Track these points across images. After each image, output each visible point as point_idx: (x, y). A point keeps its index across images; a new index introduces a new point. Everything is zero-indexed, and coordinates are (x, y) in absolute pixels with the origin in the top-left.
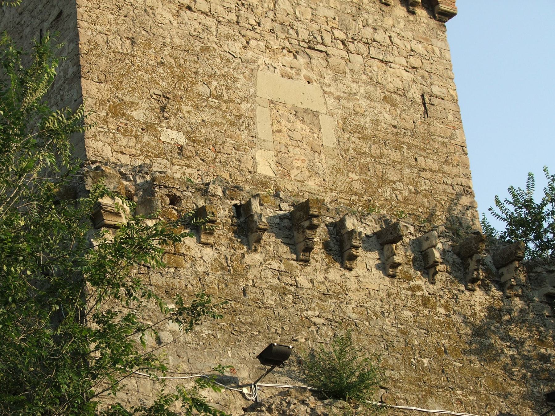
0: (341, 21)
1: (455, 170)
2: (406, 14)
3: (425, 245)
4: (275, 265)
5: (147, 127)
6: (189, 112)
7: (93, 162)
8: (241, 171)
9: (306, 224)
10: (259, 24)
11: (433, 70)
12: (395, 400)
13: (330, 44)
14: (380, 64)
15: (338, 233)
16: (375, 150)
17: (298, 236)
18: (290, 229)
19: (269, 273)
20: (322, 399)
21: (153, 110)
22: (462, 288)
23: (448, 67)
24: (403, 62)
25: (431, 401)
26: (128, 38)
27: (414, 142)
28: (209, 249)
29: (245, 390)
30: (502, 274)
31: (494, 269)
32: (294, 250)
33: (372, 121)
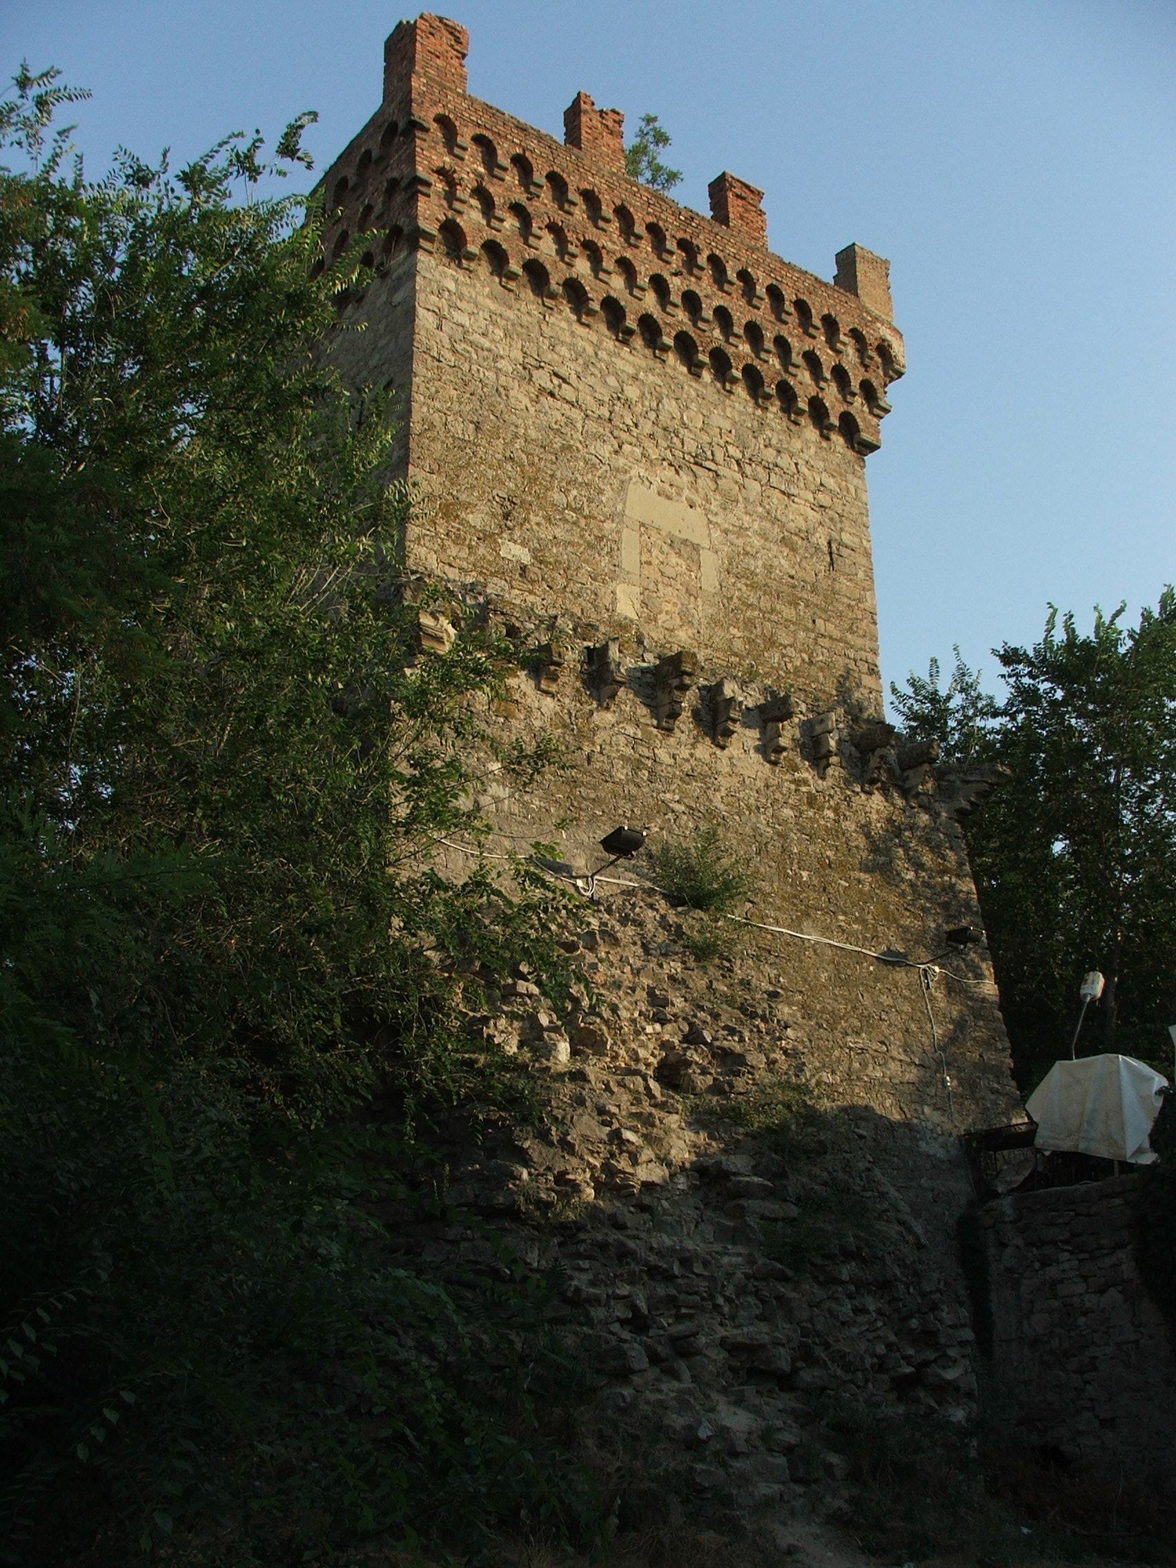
0: (738, 436)
1: (860, 642)
2: (819, 439)
3: (818, 729)
4: (631, 730)
5: (486, 537)
6: (538, 524)
7: (413, 572)
8: (596, 607)
9: (675, 682)
10: (636, 426)
11: (845, 513)
12: (762, 919)
13: (721, 462)
14: (780, 495)
15: (712, 699)
16: (765, 603)
17: (663, 697)
18: (653, 687)
19: (622, 740)
20: (674, 906)
21: (494, 515)
22: (858, 789)
23: (864, 511)
24: (810, 497)
25: (806, 924)
26: (472, 422)
27: (814, 599)
28: (549, 699)
29: (580, 883)
30: (908, 778)
31: (898, 771)
32: (655, 715)
33: (764, 566)
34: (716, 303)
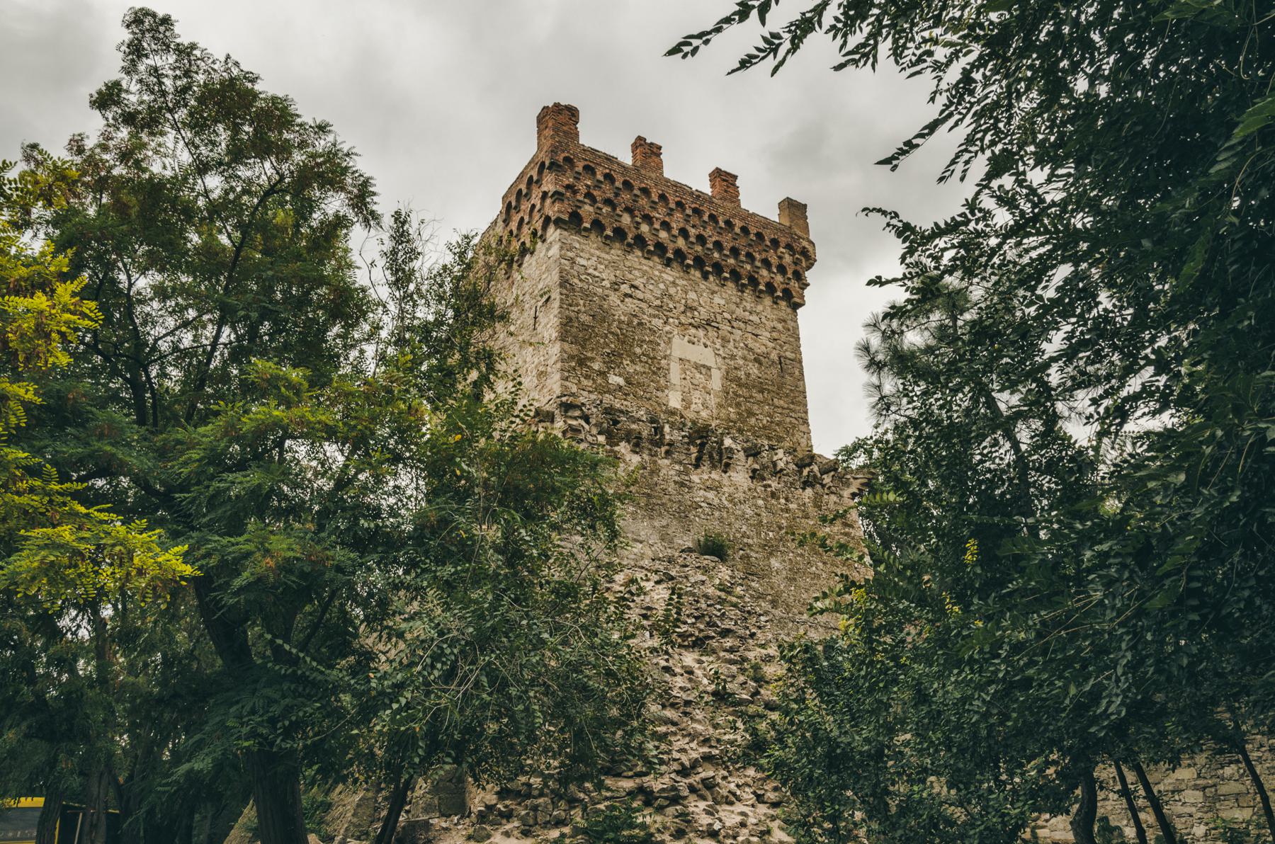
4: (677, 467)
5: (603, 374)
34: (714, 239)
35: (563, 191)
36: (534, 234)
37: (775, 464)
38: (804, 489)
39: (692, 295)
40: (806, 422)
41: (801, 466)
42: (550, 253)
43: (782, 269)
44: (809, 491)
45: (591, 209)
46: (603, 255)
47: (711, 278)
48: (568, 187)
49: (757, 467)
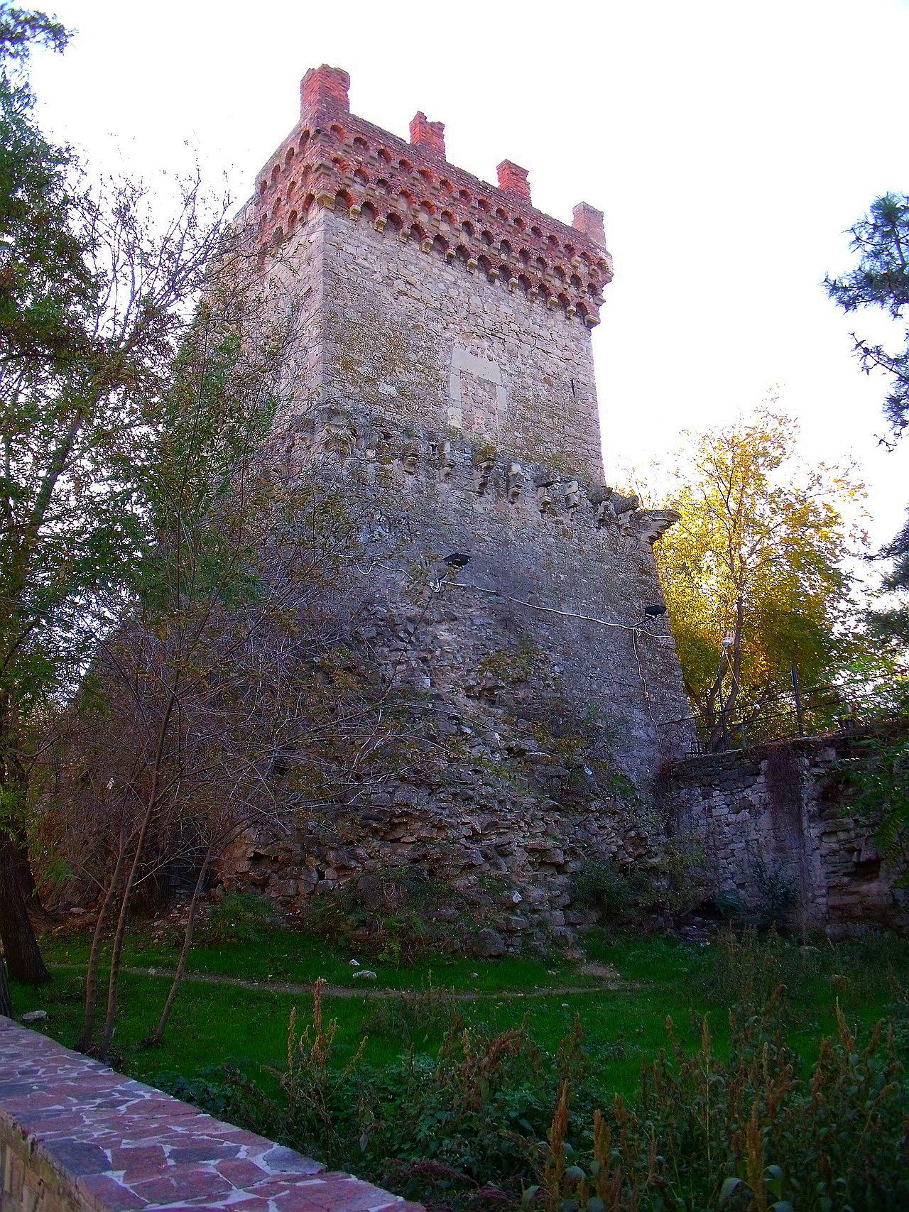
5: (370, 381)
35: (331, 165)
36: (294, 213)
37: (567, 499)
38: (598, 528)
39: (475, 300)
40: (599, 456)
41: (596, 502)
42: (313, 238)
43: (576, 280)
44: (603, 531)
45: (362, 189)
46: (375, 244)
47: (497, 283)
48: (336, 161)
49: (548, 499)
